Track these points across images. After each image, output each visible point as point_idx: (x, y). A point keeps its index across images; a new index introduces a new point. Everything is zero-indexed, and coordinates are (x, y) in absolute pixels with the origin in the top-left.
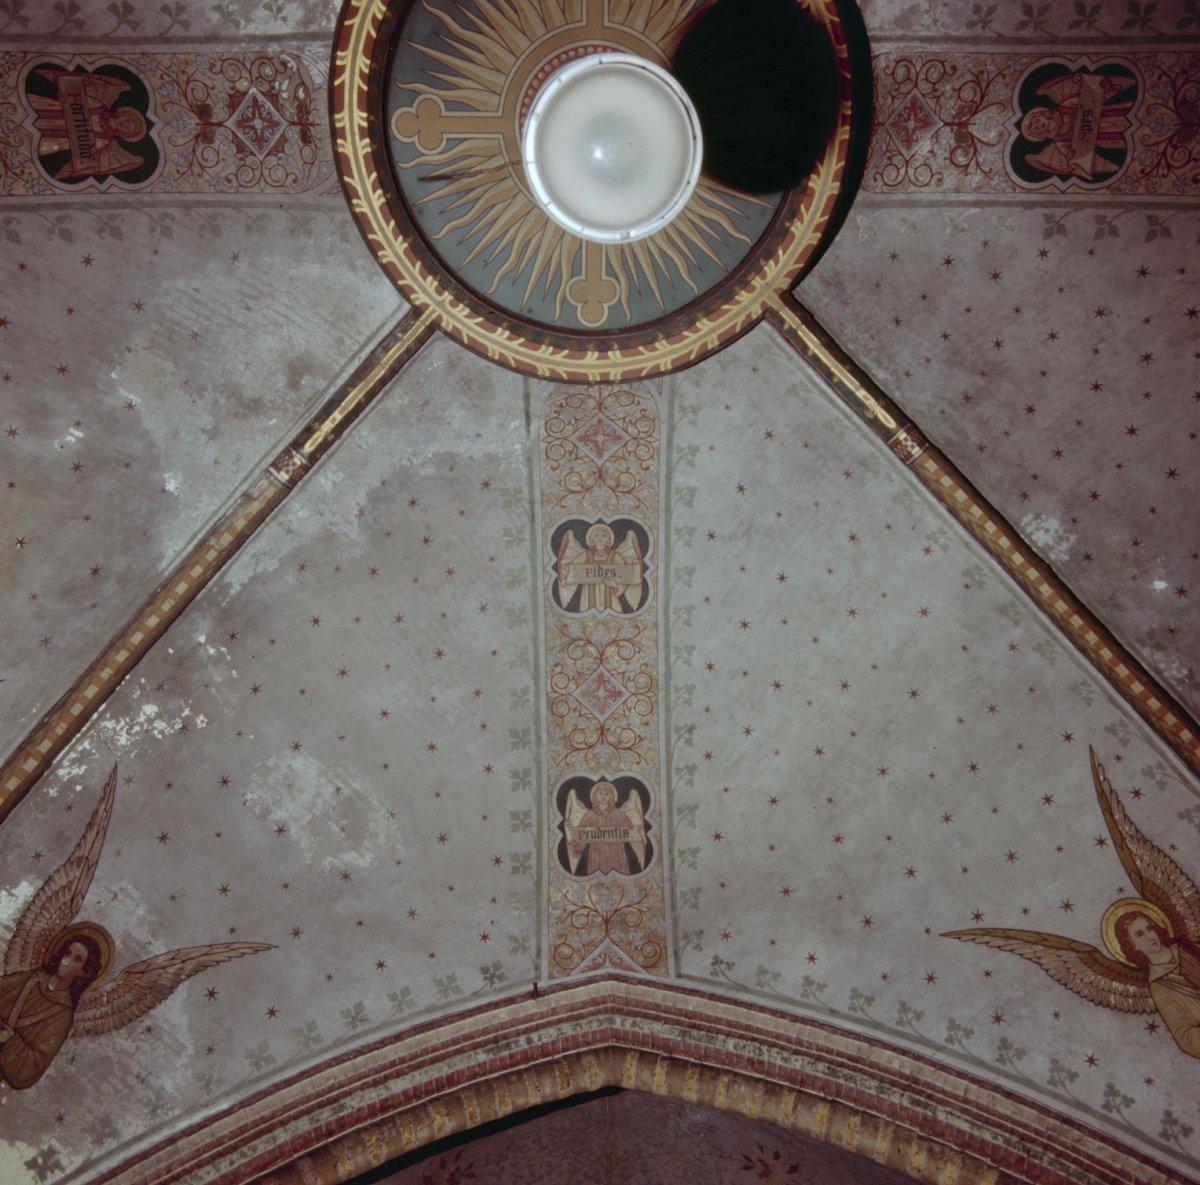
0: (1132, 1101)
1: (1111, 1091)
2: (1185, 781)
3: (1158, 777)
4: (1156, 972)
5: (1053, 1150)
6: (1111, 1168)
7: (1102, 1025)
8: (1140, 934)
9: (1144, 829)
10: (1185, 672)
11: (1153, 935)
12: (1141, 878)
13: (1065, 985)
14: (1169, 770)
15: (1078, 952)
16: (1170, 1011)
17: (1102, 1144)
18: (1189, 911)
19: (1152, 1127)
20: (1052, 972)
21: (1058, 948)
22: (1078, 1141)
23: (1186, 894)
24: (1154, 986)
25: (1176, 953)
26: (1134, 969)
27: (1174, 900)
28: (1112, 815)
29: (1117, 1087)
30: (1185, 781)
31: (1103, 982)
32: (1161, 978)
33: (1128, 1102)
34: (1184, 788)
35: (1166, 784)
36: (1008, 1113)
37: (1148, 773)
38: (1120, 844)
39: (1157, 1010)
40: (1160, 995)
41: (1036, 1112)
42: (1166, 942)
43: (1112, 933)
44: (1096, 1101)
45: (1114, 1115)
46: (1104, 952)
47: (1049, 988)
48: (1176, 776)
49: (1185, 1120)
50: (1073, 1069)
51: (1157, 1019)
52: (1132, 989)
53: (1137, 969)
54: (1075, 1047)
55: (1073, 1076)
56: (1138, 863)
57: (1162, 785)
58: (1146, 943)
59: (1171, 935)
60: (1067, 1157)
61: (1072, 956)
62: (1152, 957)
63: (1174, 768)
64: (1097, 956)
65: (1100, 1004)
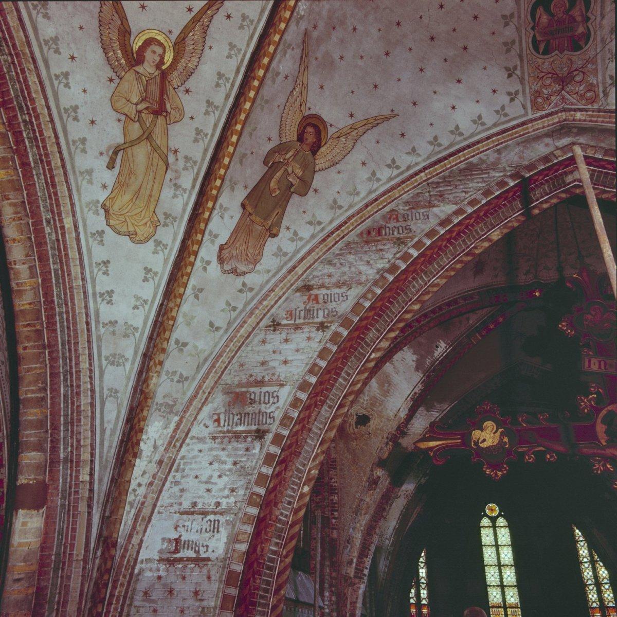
0: (69, 88)
1: (66, 75)
2: (251, 37)
3: (245, 23)
4: (139, 69)
5: (12, 58)
6: (29, 93)
7: (95, 54)
8: (154, 52)
9: (212, 29)
10: (302, 14)
11: (158, 59)
12: (184, 39)
13: (101, 25)
14: (252, 27)
15: (122, 24)
16: (125, 85)
17: (37, 82)
18: (181, 70)
19: (65, 103)
20: (102, 15)
21: (117, 12)
22: (29, 69)
23: (189, 65)
24: (132, 71)
25: (156, 74)
26: (133, 57)
27: (182, 61)
28: (208, 9)
29: (70, 77)
30: (251, 37)
31: (116, 45)
32: (138, 73)
33: (67, 86)
34: (247, 38)
35: (243, 29)
36: (11, 24)
37: (244, 17)
38: (195, 20)
39: (121, 78)
40: (130, 76)
41: (24, 40)
42: (159, 66)
43: (144, 38)
44: (55, 70)
45: (56, 83)
46: (132, 38)
47: (92, 17)
48: (251, 32)
49: (80, 115)
50: (61, 50)
51: (117, 80)
52: (123, 61)
53: (135, 59)
54: (72, 45)
55: (57, 51)
56: (191, 34)
57: (241, 27)
58: (150, 57)
59: (164, 67)
60: (15, 68)
61: (119, 22)
62: (146, 64)
63: (255, 29)
64: (127, 35)
65: (104, 49)
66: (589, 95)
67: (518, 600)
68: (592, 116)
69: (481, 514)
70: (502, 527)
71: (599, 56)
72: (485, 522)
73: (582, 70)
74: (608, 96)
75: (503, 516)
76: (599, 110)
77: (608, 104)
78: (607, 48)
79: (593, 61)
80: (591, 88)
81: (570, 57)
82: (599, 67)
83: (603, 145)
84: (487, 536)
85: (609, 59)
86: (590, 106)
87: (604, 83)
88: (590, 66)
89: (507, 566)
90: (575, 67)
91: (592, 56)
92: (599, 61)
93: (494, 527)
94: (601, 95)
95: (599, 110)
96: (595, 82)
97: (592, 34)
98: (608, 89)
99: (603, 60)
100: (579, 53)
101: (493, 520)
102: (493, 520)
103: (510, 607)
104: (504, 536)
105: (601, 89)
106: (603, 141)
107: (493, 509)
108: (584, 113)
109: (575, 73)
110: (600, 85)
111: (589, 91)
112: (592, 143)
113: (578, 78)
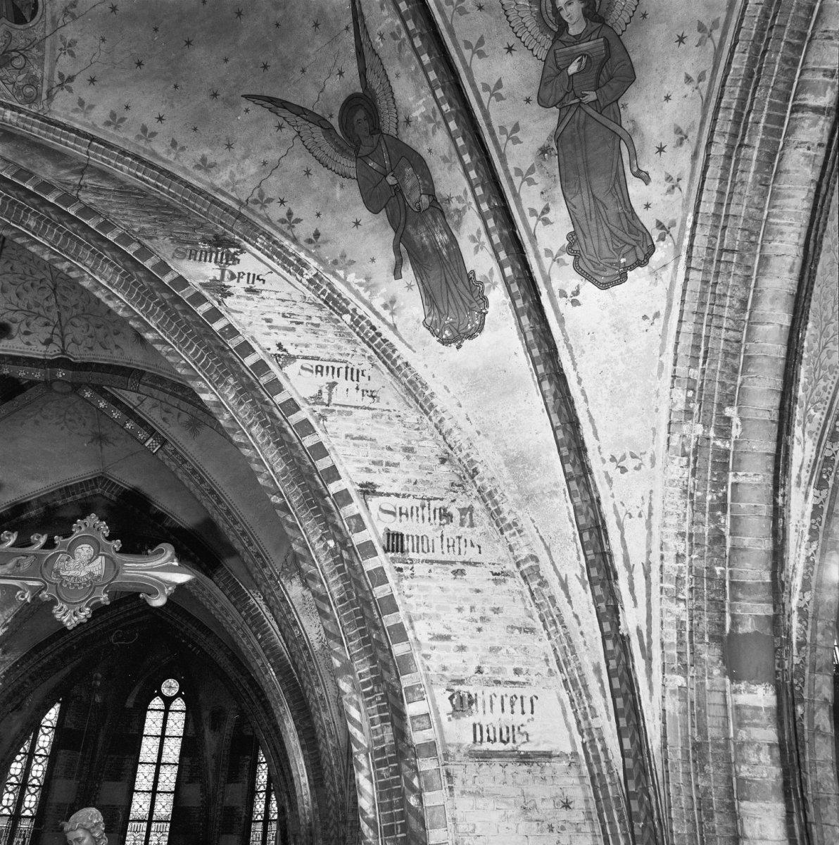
66: (28, 90)
67: (170, 812)
68: (25, 121)
69: (153, 690)
70: (177, 711)
71: (48, 41)
72: (157, 703)
73: (23, 52)
74: (52, 100)
75: (184, 698)
76: (36, 116)
77: (50, 111)
78: (58, 33)
79: (39, 45)
80: (33, 81)
81: (10, 30)
82: (47, 56)
83: (22, 163)
84: (152, 723)
85: (61, 49)
86: (26, 107)
87: (50, 80)
88: (34, 50)
89: (169, 764)
90: (14, 45)
91: (38, 38)
92: (47, 47)
93: (166, 711)
94: (44, 96)
95: (36, 116)
96: (39, 76)
97: (40, 6)
98: (54, 91)
99: (53, 49)
100: (21, 27)
101: (168, 701)
102: (168, 701)
103: (156, 821)
104: (177, 723)
105: (45, 88)
106: (24, 158)
107: (170, 687)
108: (16, 113)
109: (14, 54)
110: (45, 82)
111: (30, 85)
112: (9, 157)
113: (18, 63)
